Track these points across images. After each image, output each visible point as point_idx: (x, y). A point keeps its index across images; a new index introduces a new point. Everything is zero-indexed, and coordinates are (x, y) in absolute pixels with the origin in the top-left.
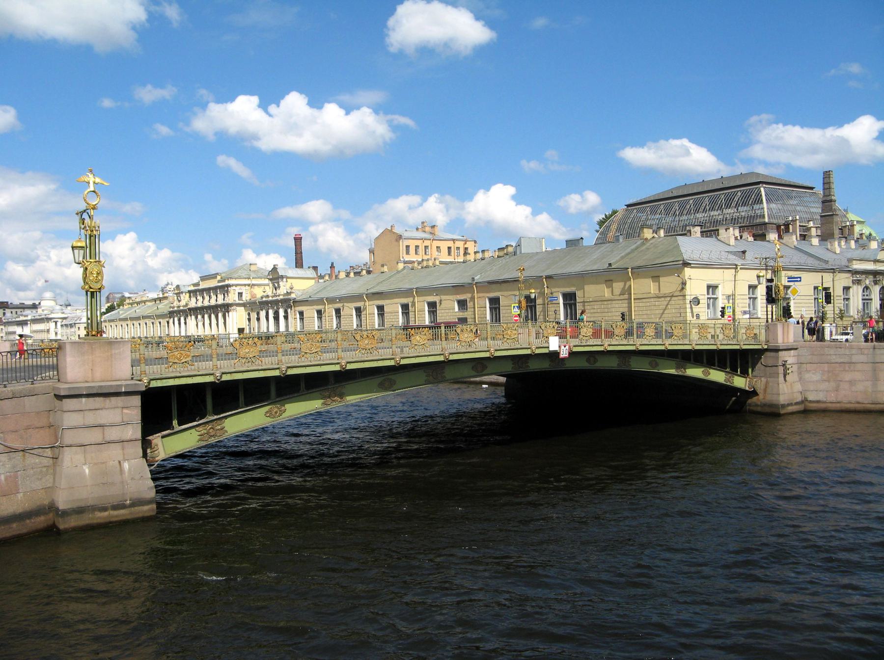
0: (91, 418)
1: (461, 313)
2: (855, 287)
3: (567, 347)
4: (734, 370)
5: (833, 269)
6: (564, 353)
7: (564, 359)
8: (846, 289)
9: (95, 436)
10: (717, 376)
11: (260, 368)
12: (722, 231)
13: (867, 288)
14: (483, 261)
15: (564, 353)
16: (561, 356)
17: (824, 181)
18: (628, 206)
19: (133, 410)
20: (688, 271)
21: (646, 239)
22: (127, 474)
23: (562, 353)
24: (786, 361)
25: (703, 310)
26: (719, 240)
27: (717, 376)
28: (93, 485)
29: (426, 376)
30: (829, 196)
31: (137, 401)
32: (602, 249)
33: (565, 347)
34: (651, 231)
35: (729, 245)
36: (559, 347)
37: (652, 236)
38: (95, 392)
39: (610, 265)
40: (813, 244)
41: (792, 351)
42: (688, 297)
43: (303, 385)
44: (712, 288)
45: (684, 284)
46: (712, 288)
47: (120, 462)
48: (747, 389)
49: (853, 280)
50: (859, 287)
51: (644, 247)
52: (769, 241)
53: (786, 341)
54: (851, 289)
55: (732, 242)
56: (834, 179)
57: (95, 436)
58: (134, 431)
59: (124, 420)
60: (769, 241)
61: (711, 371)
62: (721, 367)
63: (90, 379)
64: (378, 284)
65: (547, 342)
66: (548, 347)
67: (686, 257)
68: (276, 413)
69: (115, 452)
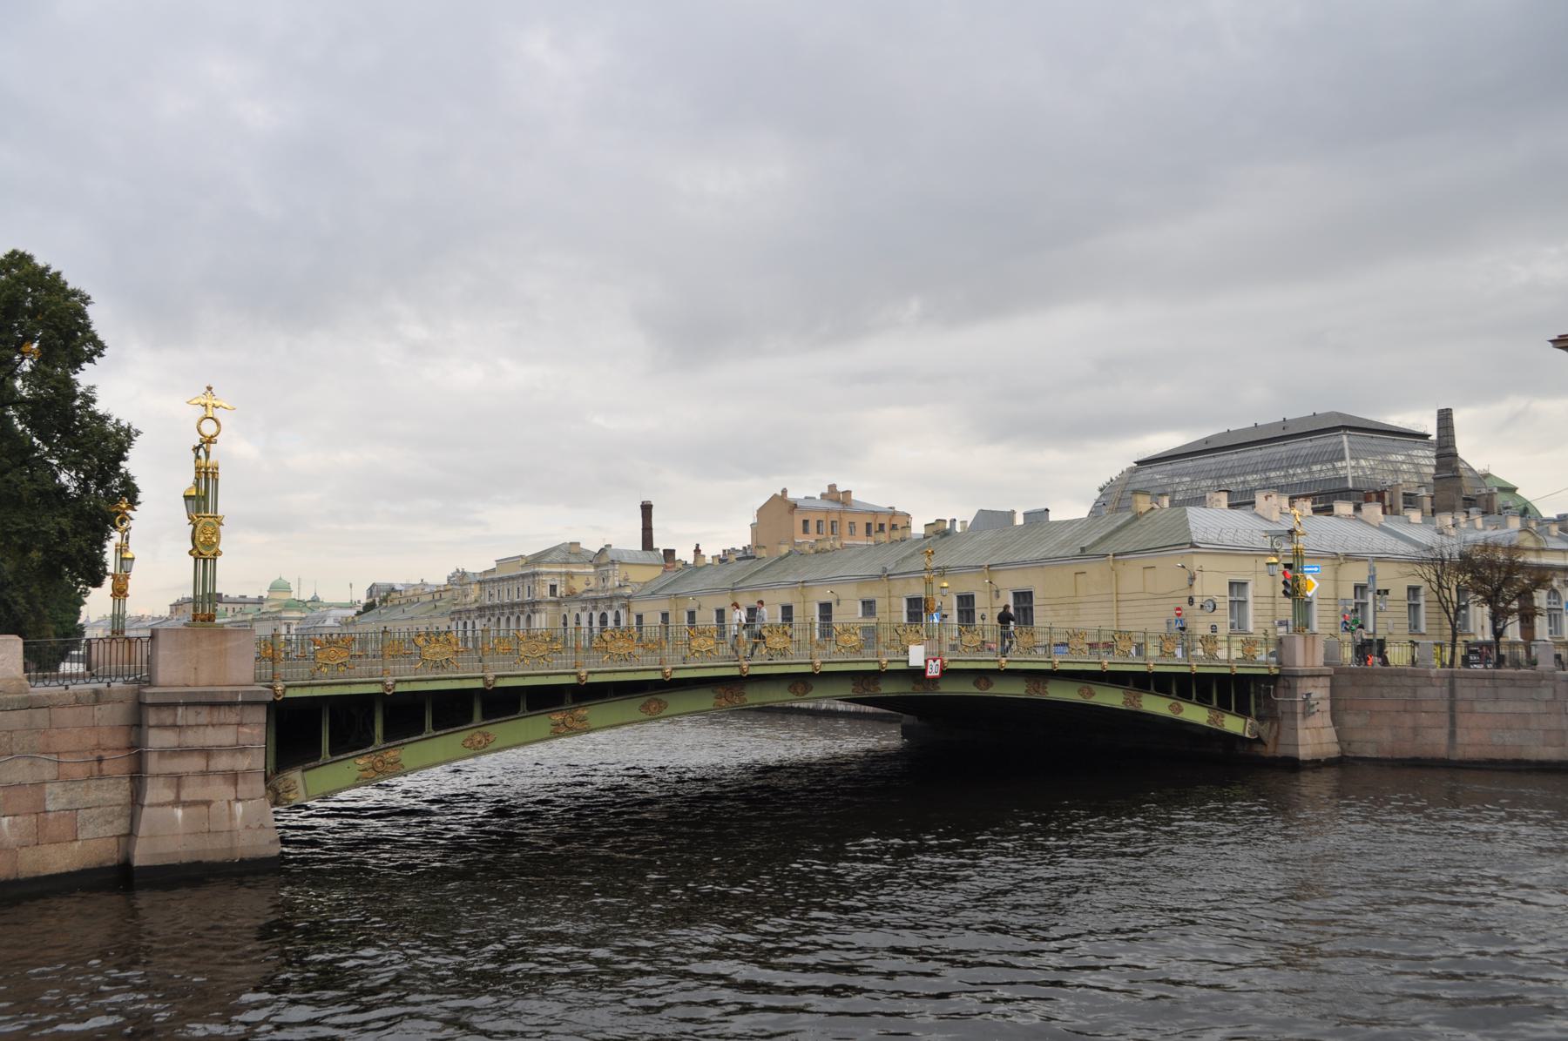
1: (866, 620)
3: (938, 662)
4: (1224, 706)
6: (933, 671)
7: (934, 679)
10: (1196, 714)
11: (454, 675)
12: (1259, 498)
14: (903, 544)
15: (933, 671)
17: (1438, 423)
18: (1138, 463)
19: (255, 731)
20: (1197, 562)
22: (239, 820)
23: (929, 670)
24: (1309, 694)
25: (1223, 619)
26: (1256, 514)
27: (1196, 714)
28: (186, 834)
29: (716, 698)
30: (1447, 447)
31: (260, 715)
33: (934, 661)
34: (1148, 498)
36: (926, 661)
37: (1149, 506)
38: (197, 699)
39: (1083, 549)
40: (1412, 521)
43: (523, 705)
44: (1237, 586)
45: (1193, 578)
46: (1237, 586)
47: (229, 802)
48: (1247, 735)
52: (1337, 516)
53: (1309, 664)
55: (1276, 516)
56: (1457, 418)
58: (256, 761)
59: (241, 742)
60: (1337, 516)
61: (1184, 705)
62: (1204, 700)
63: (192, 682)
64: (750, 576)
65: (906, 652)
66: (908, 661)
67: (1194, 539)
68: (480, 742)
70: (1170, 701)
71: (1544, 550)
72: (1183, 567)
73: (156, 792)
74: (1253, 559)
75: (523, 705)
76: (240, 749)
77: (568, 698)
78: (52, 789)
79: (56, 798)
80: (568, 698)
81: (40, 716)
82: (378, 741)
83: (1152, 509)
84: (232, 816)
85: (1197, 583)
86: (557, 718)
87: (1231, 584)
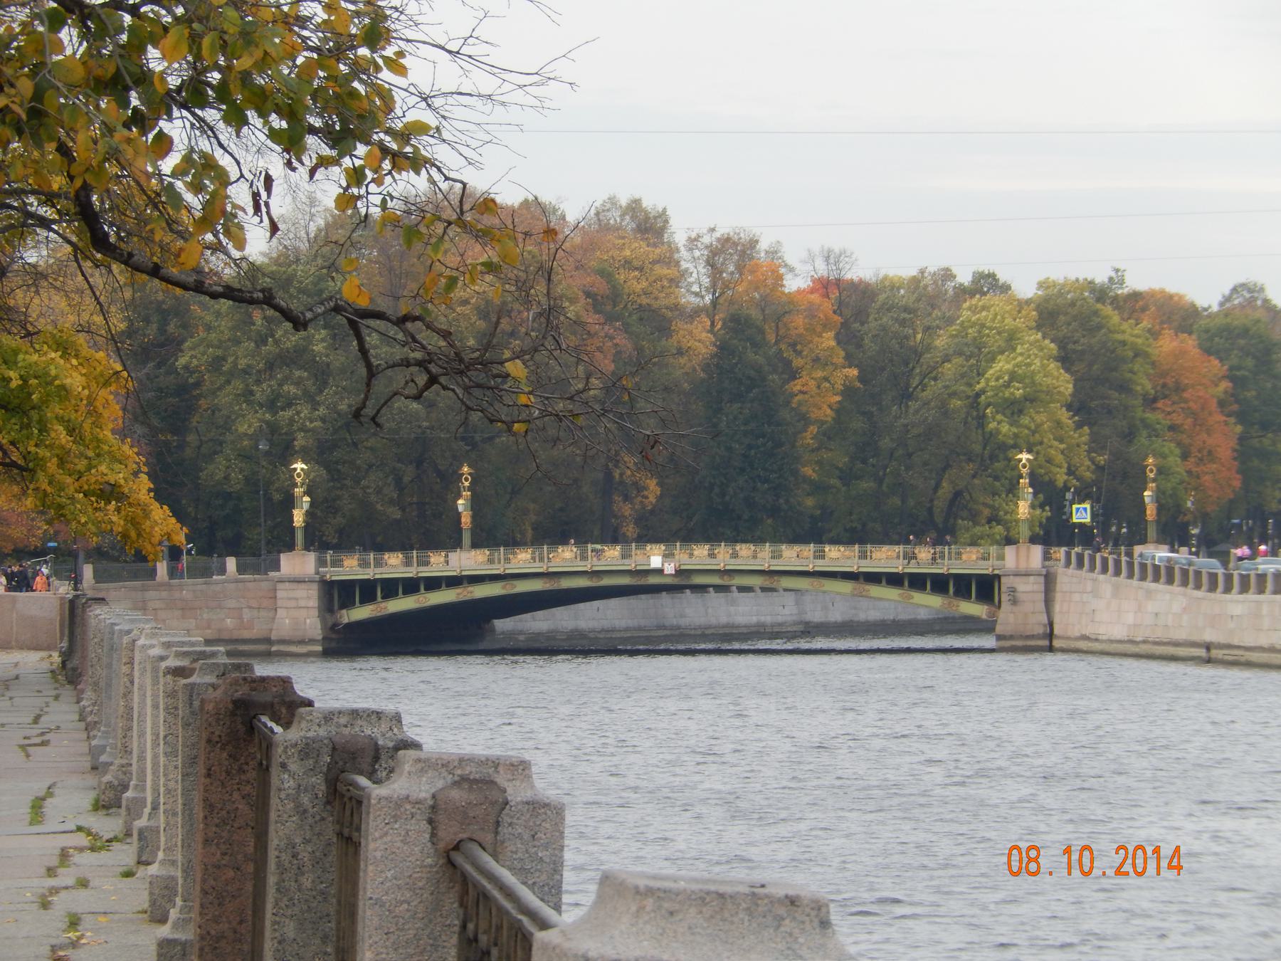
0: (292, 594)
9: (293, 604)
16: (666, 572)
31: (315, 586)
41: (1032, 578)
43: (444, 585)
48: (984, 617)
57: (293, 604)
69: (303, 613)
70: (901, 592)
73: (281, 613)
75: (444, 585)
76: (308, 598)
77: (465, 581)
78: (245, 611)
79: (247, 615)
80: (465, 581)
81: (240, 585)
82: (379, 599)
84: (305, 623)
86: (459, 591)
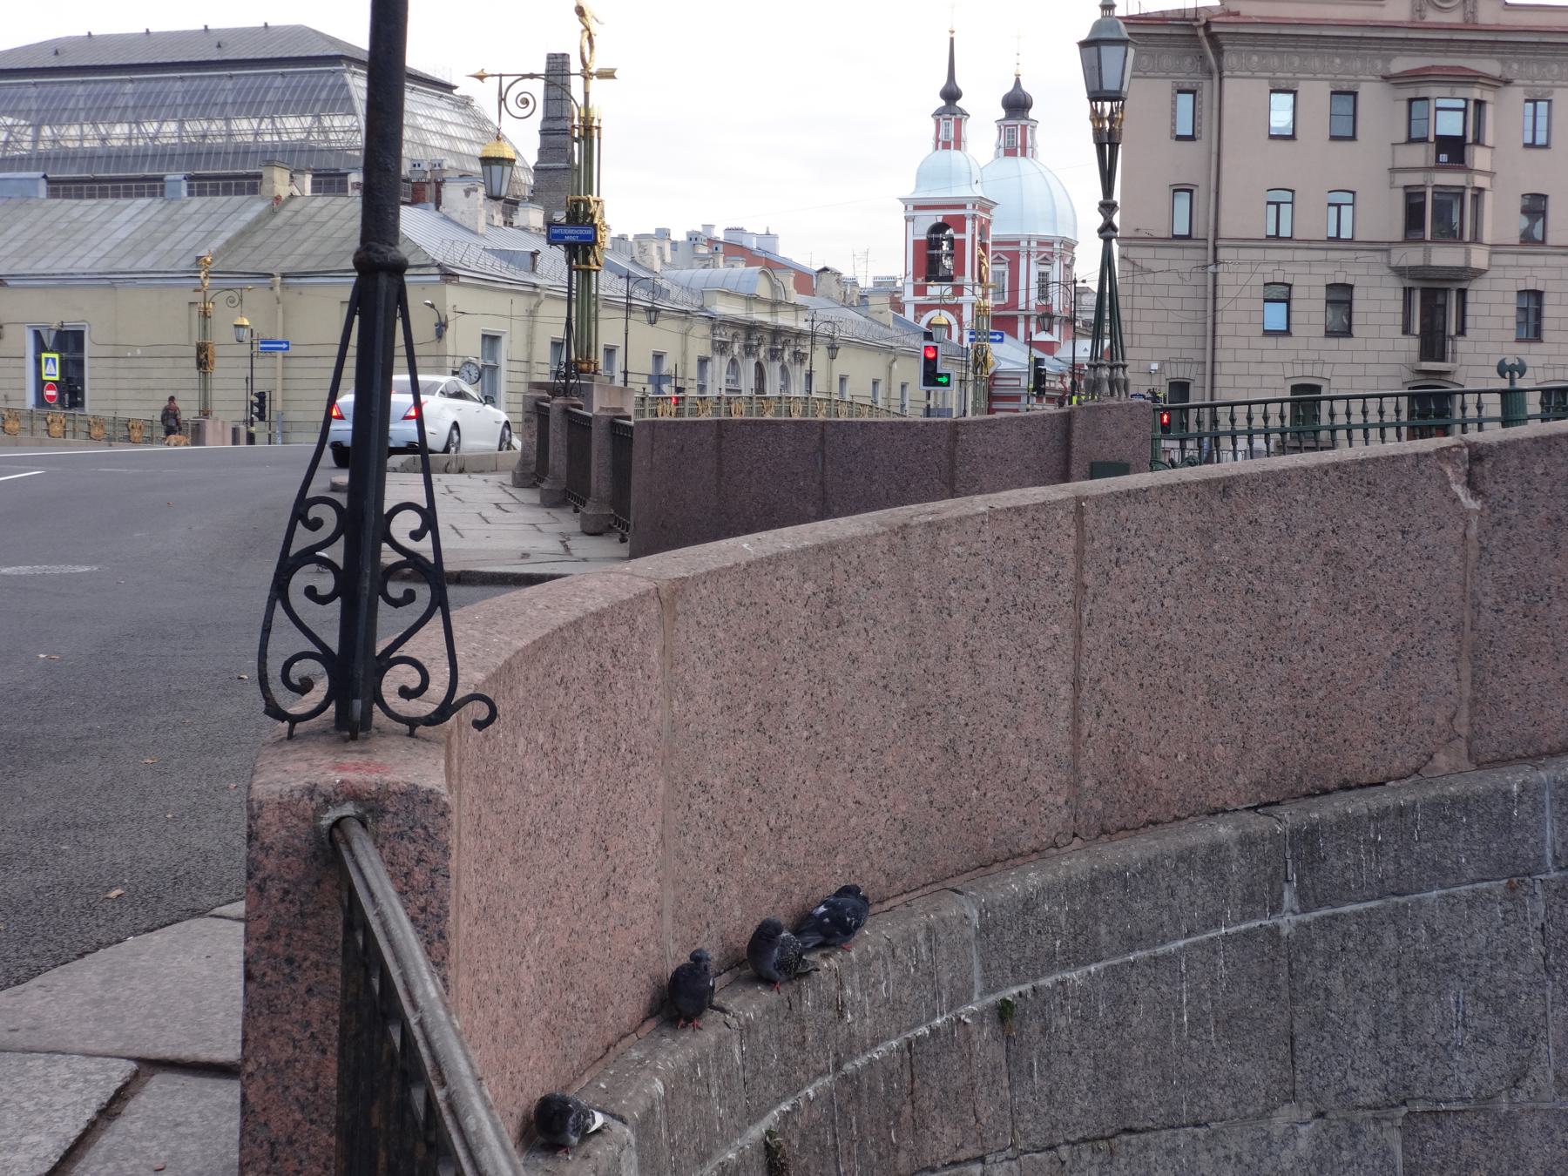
2: (717, 358)
5: (687, 312)
8: (703, 362)
13: (733, 361)
21: (278, 198)
26: (446, 218)
32: (131, 211)
35: (475, 233)
42: (449, 362)
46: (491, 340)
49: (714, 342)
50: (724, 358)
51: (278, 221)
52: (525, 229)
54: (709, 364)
60: (525, 229)
71: (780, 303)
72: (432, 306)
74: (510, 297)
83: (292, 196)
85: (449, 333)
87: (484, 336)
